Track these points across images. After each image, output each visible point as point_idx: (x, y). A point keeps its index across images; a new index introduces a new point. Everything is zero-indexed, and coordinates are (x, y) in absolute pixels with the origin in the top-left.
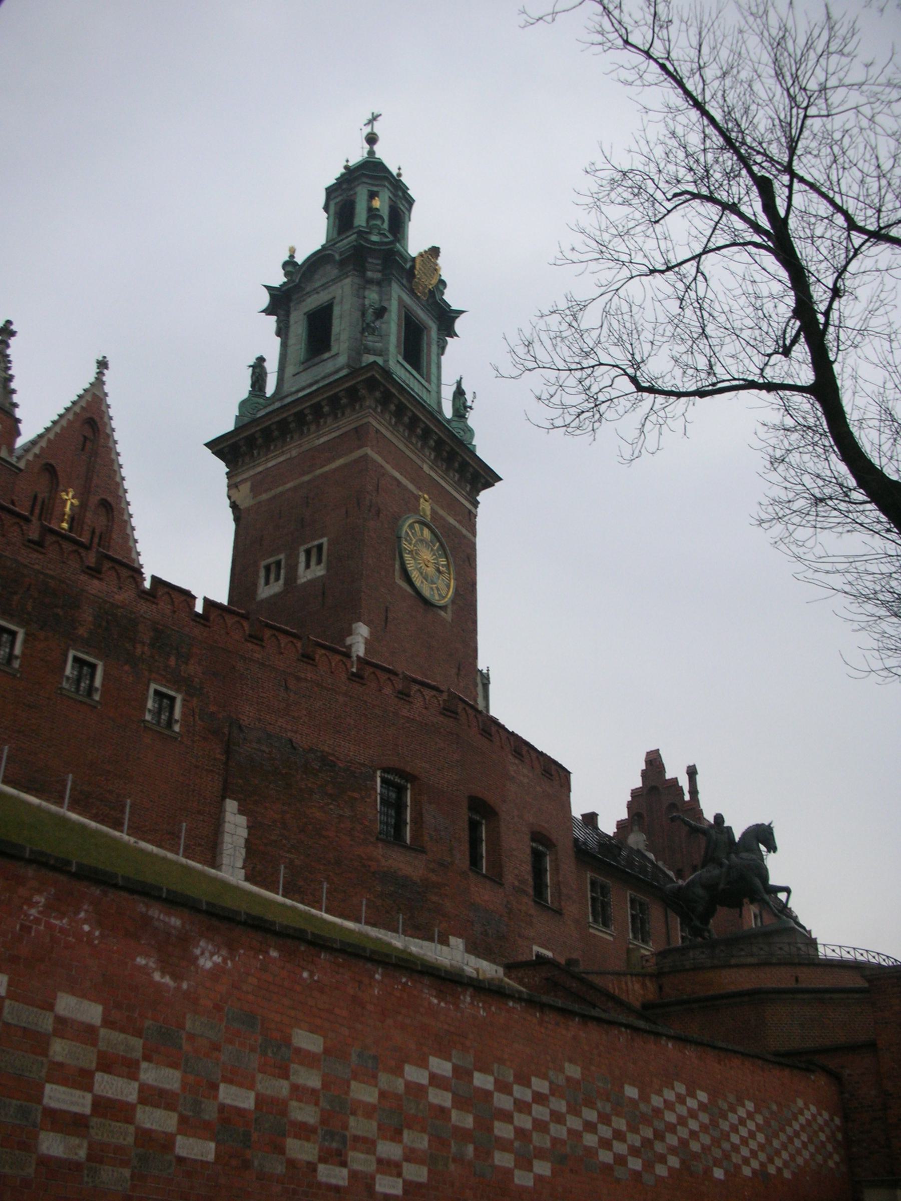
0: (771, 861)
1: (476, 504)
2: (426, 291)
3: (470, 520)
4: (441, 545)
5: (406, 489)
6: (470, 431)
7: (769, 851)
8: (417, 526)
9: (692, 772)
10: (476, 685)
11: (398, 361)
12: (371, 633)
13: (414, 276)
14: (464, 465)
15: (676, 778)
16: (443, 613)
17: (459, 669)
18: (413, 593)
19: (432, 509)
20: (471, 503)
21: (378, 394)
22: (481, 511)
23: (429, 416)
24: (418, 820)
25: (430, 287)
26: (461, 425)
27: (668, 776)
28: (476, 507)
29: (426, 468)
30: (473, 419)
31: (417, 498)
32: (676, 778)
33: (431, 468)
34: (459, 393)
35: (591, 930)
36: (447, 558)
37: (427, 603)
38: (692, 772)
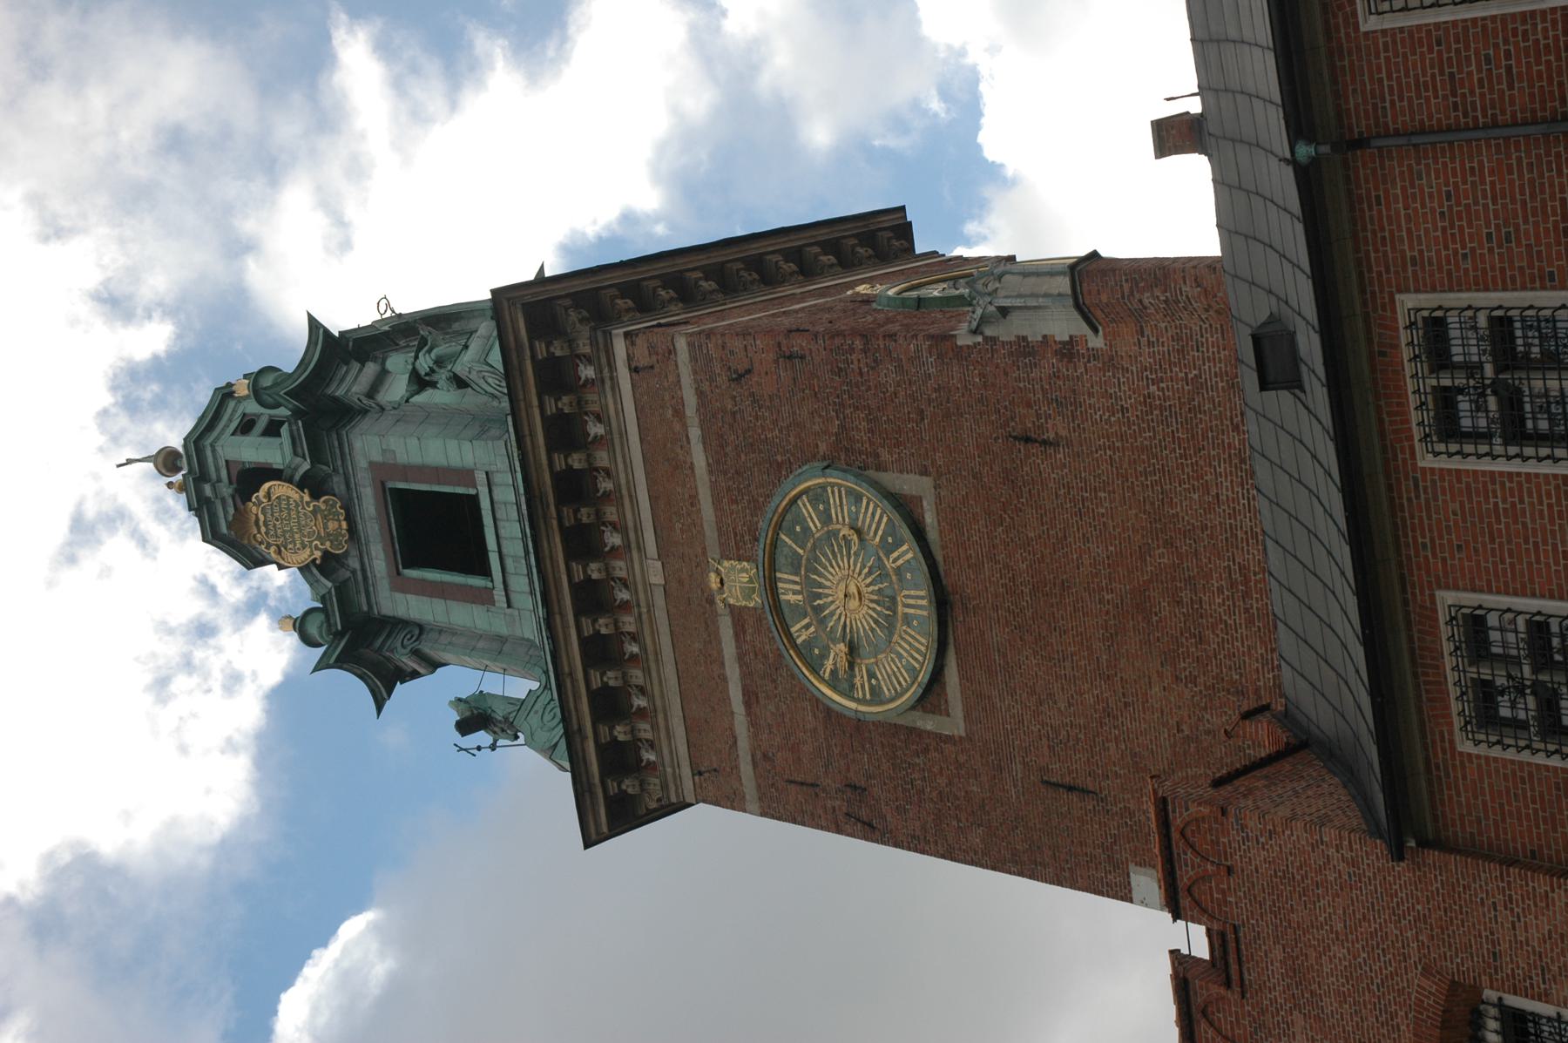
2: (321, 504)
4: (779, 527)
5: (741, 657)
8: (802, 631)
10: (1024, 349)
11: (509, 606)
12: (1141, 864)
13: (326, 555)
16: (930, 518)
17: (1028, 440)
21: (629, 785)
23: (558, 618)
25: (307, 498)
29: (656, 576)
31: (737, 614)
33: (641, 548)
36: (794, 501)
37: (943, 602)
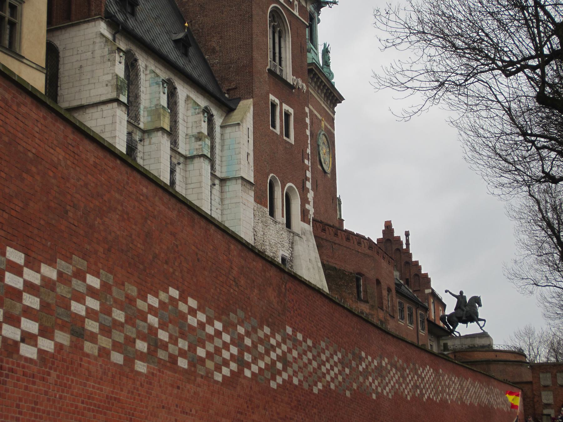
0: (480, 310)
1: (334, 113)
3: (331, 121)
6: (331, 73)
7: (479, 306)
9: (407, 234)
14: (334, 96)
15: (400, 237)
18: (321, 169)
19: (325, 124)
20: (332, 112)
22: (336, 116)
24: (365, 291)
26: (328, 71)
27: (395, 235)
28: (334, 115)
30: (333, 67)
31: (321, 121)
32: (400, 237)
34: (326, 52)
35: (399, 322)
37: (325, 172)
38: (407, 234)
